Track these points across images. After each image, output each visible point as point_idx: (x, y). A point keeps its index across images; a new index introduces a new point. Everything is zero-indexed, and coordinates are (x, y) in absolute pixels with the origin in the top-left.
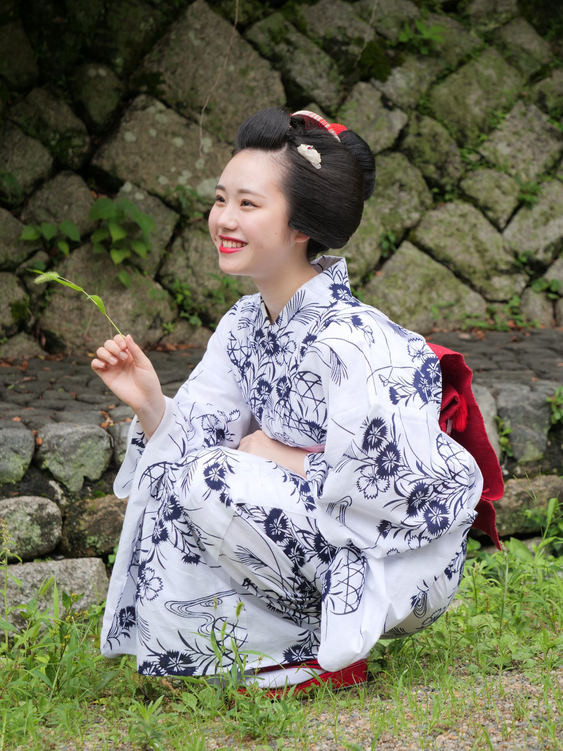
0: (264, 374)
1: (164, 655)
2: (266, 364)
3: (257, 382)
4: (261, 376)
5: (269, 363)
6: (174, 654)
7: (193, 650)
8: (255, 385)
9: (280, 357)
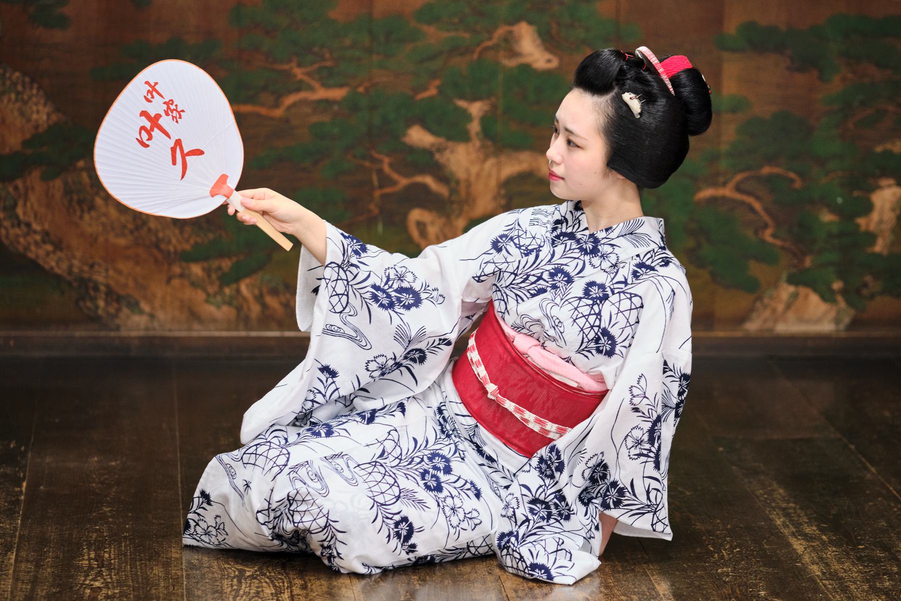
0: (566, 265)
2: (575, 258)
3: (553, 266)
4: (562, 265)
5: (578, 258)
8: (549, 267)
9: (596, 261)
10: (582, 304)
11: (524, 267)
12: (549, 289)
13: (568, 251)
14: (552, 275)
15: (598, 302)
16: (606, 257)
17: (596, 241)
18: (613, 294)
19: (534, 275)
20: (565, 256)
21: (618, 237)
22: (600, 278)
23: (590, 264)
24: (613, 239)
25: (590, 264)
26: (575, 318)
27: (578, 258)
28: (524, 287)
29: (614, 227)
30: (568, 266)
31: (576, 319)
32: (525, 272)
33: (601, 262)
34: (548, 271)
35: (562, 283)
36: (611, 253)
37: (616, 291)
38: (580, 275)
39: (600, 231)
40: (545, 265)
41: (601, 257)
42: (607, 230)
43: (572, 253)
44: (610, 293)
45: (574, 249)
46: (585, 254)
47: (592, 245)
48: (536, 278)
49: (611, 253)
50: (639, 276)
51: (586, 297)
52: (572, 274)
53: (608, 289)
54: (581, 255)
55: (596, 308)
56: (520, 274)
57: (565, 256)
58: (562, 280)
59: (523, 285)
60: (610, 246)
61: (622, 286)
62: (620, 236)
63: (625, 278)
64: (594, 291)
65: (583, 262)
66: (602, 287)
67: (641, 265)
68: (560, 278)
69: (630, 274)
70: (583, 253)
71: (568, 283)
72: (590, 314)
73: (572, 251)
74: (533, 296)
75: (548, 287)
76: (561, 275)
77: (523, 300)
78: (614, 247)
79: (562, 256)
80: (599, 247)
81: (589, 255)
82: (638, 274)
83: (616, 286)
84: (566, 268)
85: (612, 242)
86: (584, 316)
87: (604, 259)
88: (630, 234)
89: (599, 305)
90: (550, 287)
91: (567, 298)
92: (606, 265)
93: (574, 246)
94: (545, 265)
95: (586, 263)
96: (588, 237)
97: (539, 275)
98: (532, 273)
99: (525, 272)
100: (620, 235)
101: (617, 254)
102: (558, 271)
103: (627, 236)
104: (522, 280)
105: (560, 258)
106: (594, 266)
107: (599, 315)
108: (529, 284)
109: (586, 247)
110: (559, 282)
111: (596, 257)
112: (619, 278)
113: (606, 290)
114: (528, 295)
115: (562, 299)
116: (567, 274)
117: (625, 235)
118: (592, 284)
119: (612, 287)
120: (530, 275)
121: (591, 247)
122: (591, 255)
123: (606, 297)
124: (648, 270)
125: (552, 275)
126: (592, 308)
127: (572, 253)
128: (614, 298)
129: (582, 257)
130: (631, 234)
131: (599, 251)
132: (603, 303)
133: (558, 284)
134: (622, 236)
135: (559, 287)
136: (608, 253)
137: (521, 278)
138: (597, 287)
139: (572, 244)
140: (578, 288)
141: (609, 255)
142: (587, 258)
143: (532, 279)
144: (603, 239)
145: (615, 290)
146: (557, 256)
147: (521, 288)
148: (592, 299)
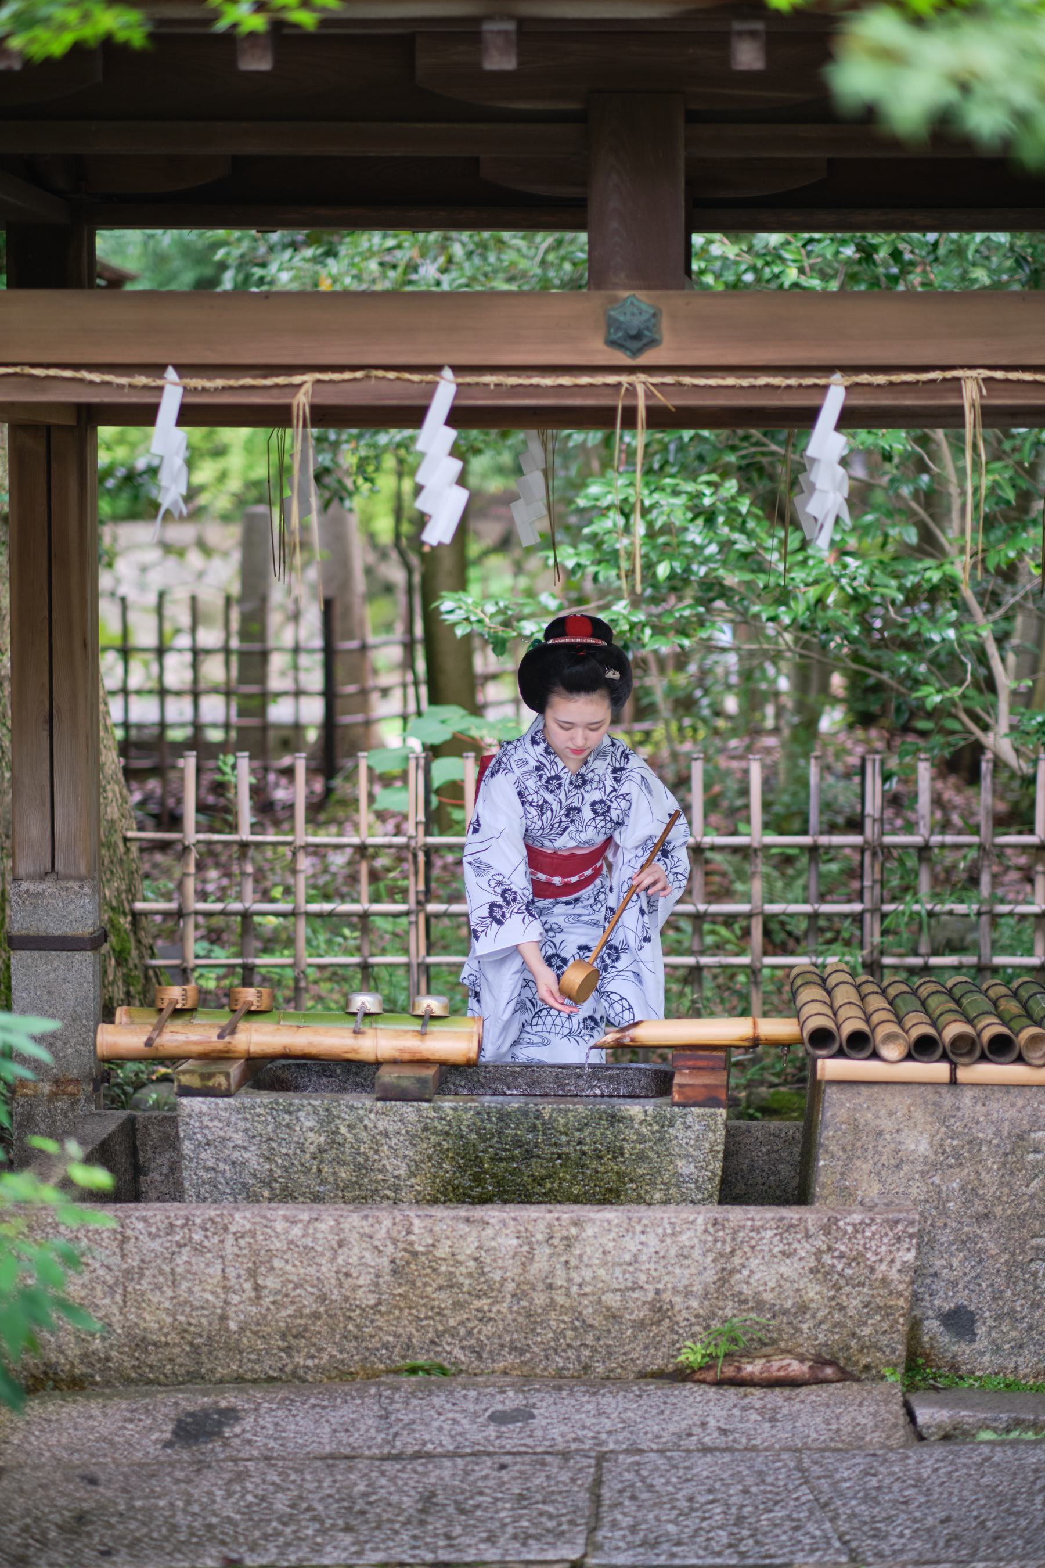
9: (588, 787)
14: (567, 815)
17: (582, 776)
22: (597, 796)
66: (602, 802)
92: (595, 785)
102: (570, 809)
107: (611, 820)
112: (609, 789)
118: (593, 804)
123: (609, 807)
125: (567, 815)
128: (614, 805)
140: (587, 813)
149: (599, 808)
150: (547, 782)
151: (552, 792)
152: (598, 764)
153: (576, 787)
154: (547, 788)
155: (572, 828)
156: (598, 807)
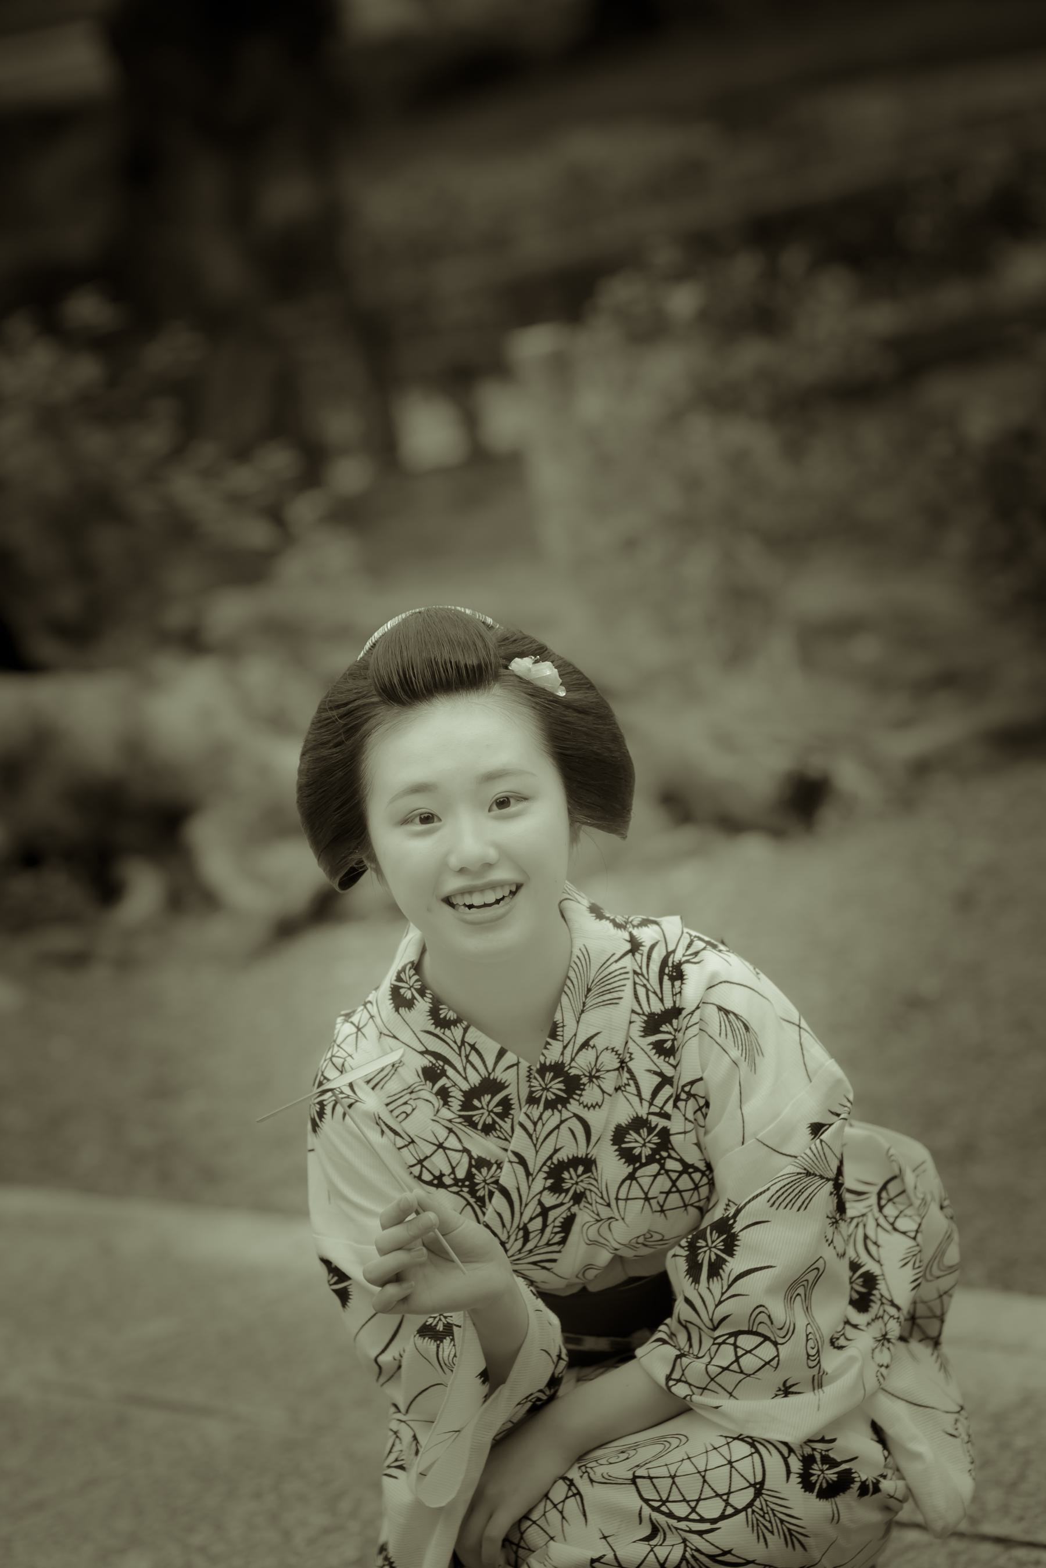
0: (556, 1151)
1: (732, 1226)
2: (558, 1127)
3: (542, 1175)
4: (550, 1157)
5: (562, 1122)
6: (730, 1246)
7: (730, 1286)
8: (540, 1182)
9: (591, 1094)
10: (645, 1182)
11: (504, 1226)
12: (574, 1209)
13: (535, 1130)
14: (556, 1188)
15: (664, 1154)
16: (598, 1071)
17: (558, 1069)
18: (667, 1116)
19: (531, 1219)
20: (540, 1140)
21: (578, 1022)
22: (623, 1110)
23: (589, 1109)
24: (575, 1035)
25: (589, 1109)
26: (659, 1209)
27: (562, 1122)
28: (536, 1247)
29: (558, 1017)
30: (560, 1149)
31: (662, 1207)
32: (513, 1229)
33: (599, 1087)
34: (545, 1189)
35: (582, 1181)
36: (597, 1058)
37: (669, 1108)
38: (593, 1139)
39: (546, 1048)
40: (529, 1187)
41: (591, 1081)
42: (553, 1035)
43: (543, 1125)
44: (663, 1123)
45: (540, 1118)
46: (564, 1106)
47: (559, 1082)
48: (539, 1220)
49: (597, 1058)
50: (673, 1045)
51: (637, 1165)
52: (581, 1153)
53: (654, 1120)
54: (560, 1112)
55: (672, 1165)
56: (509, 1237)
57: (540, 1140)
58: (578, 1176)
59: (530, 1245)
60: (584, 1050)
61: (667, 1091)
62: (579, 1018)
63: (655, 1073)
64: (639, 1143)
65: (574, 1118)
66: (638, 1123)
67: (653, 1024)
68: (571, 1178)
69: (655, 1058)
70: (560, 1107)
71: (590, 1171)
72: (674, 1183)
73: (540, 1124)
74: (563, 1242)
75: (569, 1209)
76: (569, 1173)
77: (554, 1261)
78: (591, 1043)
79: (535, 1145)
80: (573, 1072)
81: (571, 1101)
82: (668, 1045)
83: (659, 1101)
84: (562, 1156)
85: (580, 1040)
86: (668, 1193)
87: (598, 1078)
88: (588, 993)
89: (670, 1156)
90: (573, 1205)
91: (613, 1196)
92: (609, 1082)
93: (535, 1112)
94: (529, 1187)
95: (581, 1115)
96: (539, 1079)
97: (539, 1210)
98: (525, 1219)
99: (513, 1229)
100: (577, 1015)
101: (607, 1049)
102: (556, 1173)
103: (590, 1002)
104: (520, 1243)
105: (537, 1152)
106: (597, 1104)
107: (687, 1168)
108: (540, 1235)
109: (554, 1094)
110: (577, 1183)
111: (583, 1090)
112: (647, 1083)
113: (653, 1125)
114: (556, 1248)
115: (609, 1205)
116: (574, 1162)
117: (584, 1003)
118: (619, 1135)
119: (657, 1110)
120: (525, 1225)
121: (561, 1086)
122: (575, 1096)
124: (675, 1022)
125: (556, 1188)
126: (667, 1172)
127: (543, 1125)
129: (566, 1114)
130: (589, 990)
131: (578, 1077)
132: (670, 1146)
133: (579, 1189)
134: (583, 1011)
135: (585, 1189)
136: (593, 1064)
137: (516, 1240)
138: (631, 1132)
139: (528, 1112)
141: (598, 1065)
142: (574, 1106)
143: (538, 1223)
144: (562, 1054)
145: (665, 1108)
146: (529, 1155)
147: (531, 1251)
148: (650, 1160)
149: (634, 1141)
150: (467, 1105)
151: (488, 1129)
152: (594, 1021)
153: (550, 1105)
154: (472, 1124)
155: (583, 1216)
156: (634, 1141)
